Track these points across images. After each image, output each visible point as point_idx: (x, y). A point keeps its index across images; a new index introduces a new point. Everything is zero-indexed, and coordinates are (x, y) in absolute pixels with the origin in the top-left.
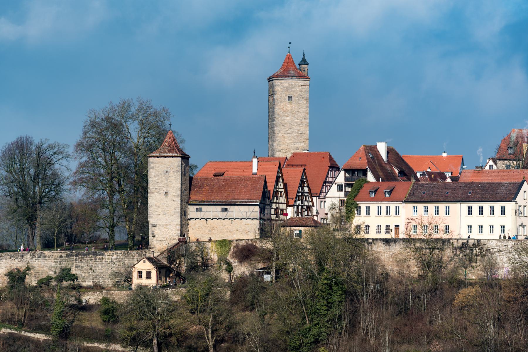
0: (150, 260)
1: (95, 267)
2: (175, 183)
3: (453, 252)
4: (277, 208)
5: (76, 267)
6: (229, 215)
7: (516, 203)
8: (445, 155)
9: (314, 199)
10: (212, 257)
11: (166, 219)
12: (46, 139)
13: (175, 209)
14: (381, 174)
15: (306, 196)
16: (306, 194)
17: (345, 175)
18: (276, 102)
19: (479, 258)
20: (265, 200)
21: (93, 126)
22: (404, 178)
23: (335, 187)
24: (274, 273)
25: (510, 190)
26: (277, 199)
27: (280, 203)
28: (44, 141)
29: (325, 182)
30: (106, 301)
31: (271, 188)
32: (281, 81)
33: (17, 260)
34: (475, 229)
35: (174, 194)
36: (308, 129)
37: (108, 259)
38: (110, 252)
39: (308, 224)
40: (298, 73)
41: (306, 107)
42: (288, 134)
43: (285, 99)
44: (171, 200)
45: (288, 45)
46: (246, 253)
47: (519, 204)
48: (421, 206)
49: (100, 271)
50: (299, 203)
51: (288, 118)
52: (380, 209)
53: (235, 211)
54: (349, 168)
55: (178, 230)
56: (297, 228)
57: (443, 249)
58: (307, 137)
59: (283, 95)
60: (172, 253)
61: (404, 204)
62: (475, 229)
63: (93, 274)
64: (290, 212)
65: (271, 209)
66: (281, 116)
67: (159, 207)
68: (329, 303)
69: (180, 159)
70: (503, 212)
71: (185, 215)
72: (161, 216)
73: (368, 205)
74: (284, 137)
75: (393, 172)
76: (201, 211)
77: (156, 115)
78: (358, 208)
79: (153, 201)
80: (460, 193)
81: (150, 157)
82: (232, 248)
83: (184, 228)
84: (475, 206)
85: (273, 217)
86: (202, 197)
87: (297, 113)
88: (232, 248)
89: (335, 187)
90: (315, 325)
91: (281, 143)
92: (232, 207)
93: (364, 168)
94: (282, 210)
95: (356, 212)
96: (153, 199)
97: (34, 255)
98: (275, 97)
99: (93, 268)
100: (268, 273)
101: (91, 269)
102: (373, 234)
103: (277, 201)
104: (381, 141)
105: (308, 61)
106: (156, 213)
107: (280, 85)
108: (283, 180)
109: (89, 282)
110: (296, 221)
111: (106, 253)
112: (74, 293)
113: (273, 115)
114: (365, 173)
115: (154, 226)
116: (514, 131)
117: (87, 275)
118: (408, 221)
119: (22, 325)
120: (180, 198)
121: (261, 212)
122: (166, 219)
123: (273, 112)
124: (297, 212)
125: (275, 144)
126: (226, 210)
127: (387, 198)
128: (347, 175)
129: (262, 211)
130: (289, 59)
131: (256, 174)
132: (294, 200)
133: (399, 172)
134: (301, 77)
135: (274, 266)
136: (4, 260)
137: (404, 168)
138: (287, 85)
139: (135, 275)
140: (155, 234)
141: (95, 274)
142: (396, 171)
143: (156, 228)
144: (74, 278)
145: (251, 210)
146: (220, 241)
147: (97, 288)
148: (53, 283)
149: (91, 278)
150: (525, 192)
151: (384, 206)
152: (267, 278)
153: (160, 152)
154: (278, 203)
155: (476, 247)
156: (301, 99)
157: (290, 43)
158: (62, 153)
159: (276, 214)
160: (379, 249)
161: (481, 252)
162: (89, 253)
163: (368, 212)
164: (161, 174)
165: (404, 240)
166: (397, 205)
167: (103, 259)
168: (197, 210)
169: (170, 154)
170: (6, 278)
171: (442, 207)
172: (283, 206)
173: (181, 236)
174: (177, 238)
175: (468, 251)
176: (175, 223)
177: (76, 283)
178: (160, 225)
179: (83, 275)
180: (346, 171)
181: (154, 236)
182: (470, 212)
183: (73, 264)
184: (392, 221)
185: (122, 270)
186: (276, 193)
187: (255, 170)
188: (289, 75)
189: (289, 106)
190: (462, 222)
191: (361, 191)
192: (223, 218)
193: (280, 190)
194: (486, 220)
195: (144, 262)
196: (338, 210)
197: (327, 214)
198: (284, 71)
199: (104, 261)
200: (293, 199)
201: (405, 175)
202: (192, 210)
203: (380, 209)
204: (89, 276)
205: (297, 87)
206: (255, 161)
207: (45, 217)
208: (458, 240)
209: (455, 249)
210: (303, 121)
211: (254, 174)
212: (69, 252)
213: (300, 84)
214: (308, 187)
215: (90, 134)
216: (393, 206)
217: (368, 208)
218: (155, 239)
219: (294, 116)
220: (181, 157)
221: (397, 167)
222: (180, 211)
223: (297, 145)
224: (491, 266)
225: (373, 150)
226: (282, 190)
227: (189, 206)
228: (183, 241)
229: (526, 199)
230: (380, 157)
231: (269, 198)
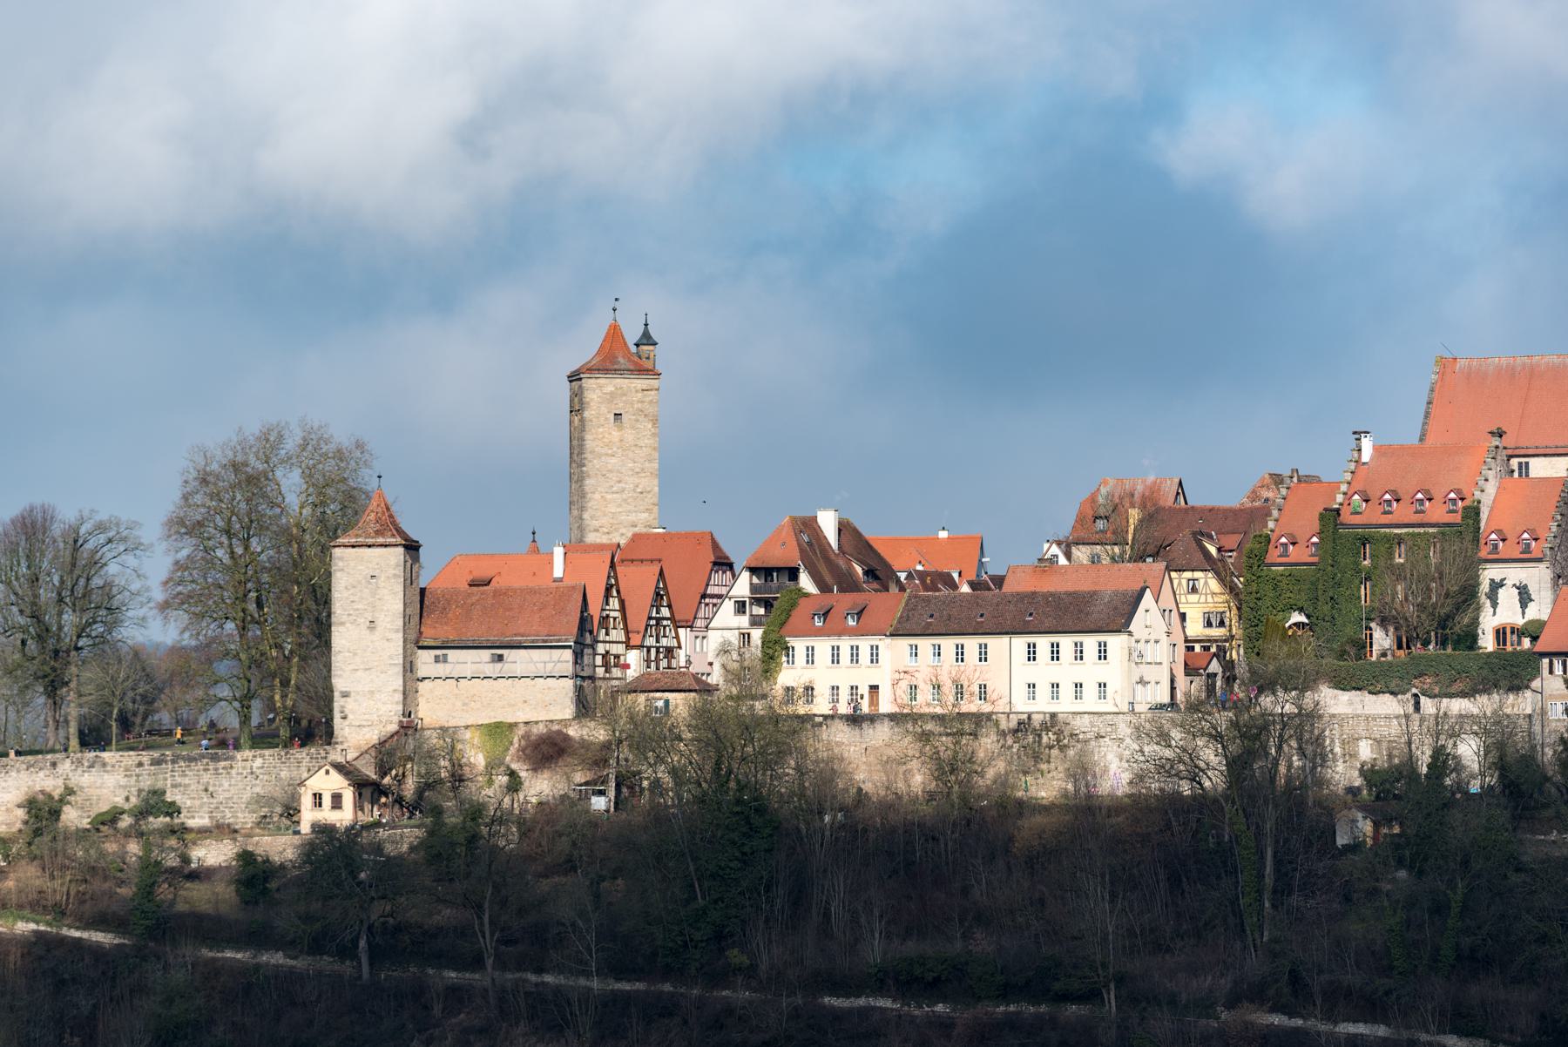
0: (339, 768)
2: (392, 603)
7: (1130, 633)
8: (943, 535)
9: (681, 631)
12: (92, 511)
13: (391, 657)
14: (828, 578)
18: (588, 424)
19: (1055, 752)
20: (584, 636)
22: (876, 585)
23: (728, 606)
24: (612, 793)
28: (86, 513)
29: (704, 596)
30: (246, 857)
31: (594, 610)
33: (41, 774)
34: (1043, 691)
36: (656, 482)
39: (682, 687)
40: (636, 364)
41: (654, 435)
45: (613, 304)
46: (548, 749)
48: (925, 644)
49: (227, 795)
50: (650, 641)
51: (613, 460)
52: (836, 651)
53: (518, 660)
54: (760, 565)
56: (658, 695)
58: (655, 500)
59: (604, 409)
60: (387, 753)
61: (888, 640)
62: (1043, 691)
64: (634, 658)
65: (595, 654)
68: (744, 854)
69: (401, 550)
70: (1103, 654)
75: (851, 573)
76: (445, 661)
77: (340, 455)
82: (516, 740)
84: (1043, 643)
85: (600, 672)
86: (446, 632)
88: (516, 740)
89: (728, 606)
90: (716, 902)
94: (617, 657)
95: (784, 659)
96: (342, 638)
97: (80, 762)
98: (586, 414)
100: (601, 793)
102: (821, 706)
104: (825, 507)
107: (598, 390)
110: (658, 680)
111: (239, 756)
112: (173, 842)
113: (581, 453)
114: (793, 574)
115: (345, 695)
117: (197, 803)
118: (897, 676)
119: (63, 913)
121: (576, 663)
123: (581, 446)
124: (648, 661)
125: (586, 516)
126: (500, 658)
128: (755, 580)
129: (578, 656)
130: (614, 333)
131: (561, 580)
133: (866, 573)
134: (643, 369)
135: (612, 777)
136: (14, 774)
137: (874, 564)
138: (610, 388)
139: (306, 801)
142: (859, 570)
144: (173, 810)
146: (489, 725)
147: (221, 830)
148: (126, 822)
151: (845, 644)
152: (599, 803)
153: (357, 536)
155: (1048, 730)
156: (641, 418)
158: (124, 539)
159: (606, 665)
160: (840, 735)
161: (1058, 741)
163: (810, 660)
165: (892, 717)
169: (381, 540)
170: (21, 813)
171: (971, 644)
174: (396, 719)
175: (1031, 739)
177: (176, 821)
180: (753, 570)
181: (344, 718)
182: (1032, 655)
184: (863, 676)
185: (278, 793)
187: (558, 571)
189: (616, 434)
190: (1019, 676)
194: (1066, 670)
195: (327, 772)
196: (735, 656)
197: (711, 664)
198: (603, 360)
199: (233, 772)
201: (876, 578)
203: (836, 651)
204: (201, 806)
206: (558, 552)
207: (85, 679)
209: (1003, 734)
211: (555, 580)
212: (156, 754)
214: (669, 606)
215: (198, 499)
216: (864, 644)
217: (810, 651)
218: (347, 722)
221: (861, 562)
223: (632, 518)
224: (1082, 771)
225: (808, 526)
226: (616, 614)
228: (408, 727)
231: (591, 632)
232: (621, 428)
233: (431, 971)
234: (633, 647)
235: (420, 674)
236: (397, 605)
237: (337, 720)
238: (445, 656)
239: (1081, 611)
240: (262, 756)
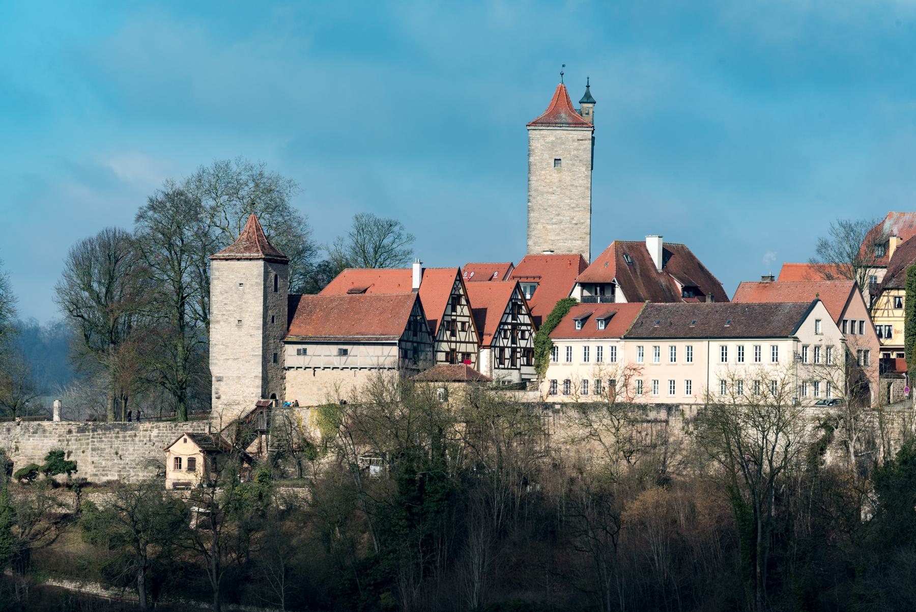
1: (123, 450)
3: (683, 428)
4: (453, 351)
5: (93, 450)
6: (350, 361)
7: (796, 339)
10: (312, 434)
11: (239, 368)
13: (253, 349)
14: (642, 292)
15: (523, 332)
16: (523, 328)
17: (582, 293)
18: (533, 168)
21: (152, 207)
25: (791, 318)
26: (453, 334)
27: (461, 342)
32: (542, 132)
35: (252, 324)
37: (144, 436)
38: (147, 425)
40: (574, 118)
42: (553, 224)
43: (548, 164)
45: (561, 69)
47: (804, 341)
48: (648, 345)
49: (132, 458)
50: (503, 342)
51: (553, 197)
54: (586, 281)
55: (257, 387)
56: (440, 384)
57: (667, 422)
59: (546, 156)
60: (246, 427)
61: (622, 343)
63: (120, 461)
65: (435, 352)
66: (542, 194)
67: (227, 347)
68: (412, 514)
69: (261, 263)
71: (275, 361)
72: (230, 362)
73: (569, 344)
74: (546, 230)
78: (553, 349)
79: (218, 336)
80: (713, 323)
81: (213, 259)
83: (271, 385)
84: (732, 346)
87: (570, 188)
91: (541, 240)
93: (609, 281)
95: (551, 357)
97: (27, 428)
99: (120, 453)
101: (117, 453)
103: (453, 339)
104: (652, 234)
105: (595, 96)
106: (225, 357)
107: (543, 140)
108: (468, 301)
109: (113, 475)
115: (220, 380)
116: (890, 215)
117: (110, 463)
118: (628, 372)
120: (261, 331)
122: (239, 368)
126: (345, 353)
127: (602, 332)
128: (586, 293)
130: (562, 95)
133: (684, 289)
137: (696, 283)
139: (170, 464)
140: (220, 393)
141: (122, 462)
142: (679, 286)
143: (221, 383)
144: (71, 467)
145: (386, 353)
149: (116, 469)
150: (817, 321)
151: (593, 345)
153: (231, 251)
154: (456, 342)
157: (563, 66)
162: (115, 426)
164: (231, 289)
166: (614, 344)
167: (135, 436)
169: (247, 255)
171: (681, 346)
172: (471, 348)
173: (263, 397)
176: (253, 375)
177: (74, 476)
178: (228, 378)
179: (104, 463)
181: (218, 398)
183: (88, 444)
186: (450, 326)
187: (416, 284)
188: (557, 121)
189: (555, 175)
191: (564, 319)
192: (341, 367)
193: (459, 319)
195: (185, 441)
198: (548, 115)
199: (137, 439)
200: (490, 335)
202: (290, 354)
205: (573, 141)
208: (691, 405)
210: (581, 201)
213: (576, 137)
216: (606, 345)
218: (220, 402)
219: (564, 194)
220: (264, 259)
221: (681, 280)
222: (261, 353)
223: (569, 244)
225: (639, 249)
226: (466, 319)
227: (287, 346)
229: (822, 334)
230: (648, 262)
232: (559, 171)
233: (193, 603)
234: (484, 347)
235: (287, 365)
236: (256, 307)
237: (214, 400)
238: (305, 350)
239: (765, 320)
240: (158, 427)
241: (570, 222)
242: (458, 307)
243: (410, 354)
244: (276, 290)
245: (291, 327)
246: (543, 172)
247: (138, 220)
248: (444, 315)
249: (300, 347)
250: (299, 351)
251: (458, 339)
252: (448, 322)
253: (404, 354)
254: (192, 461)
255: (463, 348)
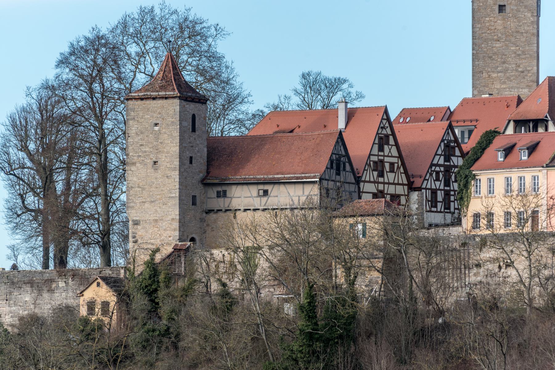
26: (381, 175)
27: (389, 183)
42: (499, 72)
44: (163, 176)
72: (147, 205)
79: (135, 179)
87: (515, 34)
92: (276, 186)
93: (541, 117)
103: (381, 180)
106: (141, 200)
122: (156, 211)
127: (526, 162)
132: (422, 179)
140: (137, 237)
145: (307, 193)
154: (384, 183)
168: (219, 195)
169: (162, 93)
172: (400, 190)
173: (180, 240)
176: (170, 217)
193: (386, 159)
195: (98, 285)
216: (528, 175)
220: (180, 98)
222: (177, 195)
226: (395, 160)
238: (225, 192)
241: (517, 70)
242: (386, 147)
243: (333, 194)
244: (194, 130)
245: (211, 169)
246: (487, 19)
247: (57, 66)
248: (370, 155)
249: (219, 189)
250: (218, 193)
251: (386, 181)
252: (375, 162)
253: (325, 193)
254: (106, 305)
255: (391, 189)
